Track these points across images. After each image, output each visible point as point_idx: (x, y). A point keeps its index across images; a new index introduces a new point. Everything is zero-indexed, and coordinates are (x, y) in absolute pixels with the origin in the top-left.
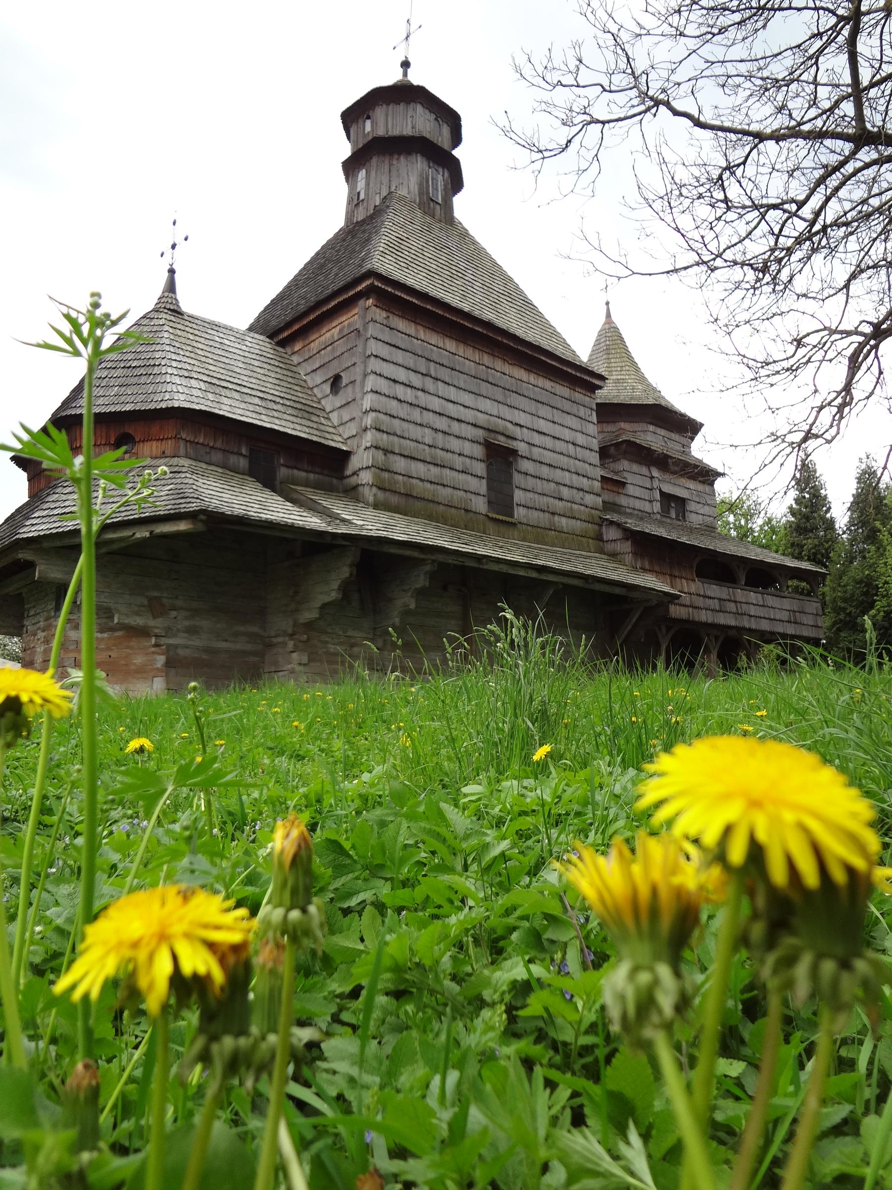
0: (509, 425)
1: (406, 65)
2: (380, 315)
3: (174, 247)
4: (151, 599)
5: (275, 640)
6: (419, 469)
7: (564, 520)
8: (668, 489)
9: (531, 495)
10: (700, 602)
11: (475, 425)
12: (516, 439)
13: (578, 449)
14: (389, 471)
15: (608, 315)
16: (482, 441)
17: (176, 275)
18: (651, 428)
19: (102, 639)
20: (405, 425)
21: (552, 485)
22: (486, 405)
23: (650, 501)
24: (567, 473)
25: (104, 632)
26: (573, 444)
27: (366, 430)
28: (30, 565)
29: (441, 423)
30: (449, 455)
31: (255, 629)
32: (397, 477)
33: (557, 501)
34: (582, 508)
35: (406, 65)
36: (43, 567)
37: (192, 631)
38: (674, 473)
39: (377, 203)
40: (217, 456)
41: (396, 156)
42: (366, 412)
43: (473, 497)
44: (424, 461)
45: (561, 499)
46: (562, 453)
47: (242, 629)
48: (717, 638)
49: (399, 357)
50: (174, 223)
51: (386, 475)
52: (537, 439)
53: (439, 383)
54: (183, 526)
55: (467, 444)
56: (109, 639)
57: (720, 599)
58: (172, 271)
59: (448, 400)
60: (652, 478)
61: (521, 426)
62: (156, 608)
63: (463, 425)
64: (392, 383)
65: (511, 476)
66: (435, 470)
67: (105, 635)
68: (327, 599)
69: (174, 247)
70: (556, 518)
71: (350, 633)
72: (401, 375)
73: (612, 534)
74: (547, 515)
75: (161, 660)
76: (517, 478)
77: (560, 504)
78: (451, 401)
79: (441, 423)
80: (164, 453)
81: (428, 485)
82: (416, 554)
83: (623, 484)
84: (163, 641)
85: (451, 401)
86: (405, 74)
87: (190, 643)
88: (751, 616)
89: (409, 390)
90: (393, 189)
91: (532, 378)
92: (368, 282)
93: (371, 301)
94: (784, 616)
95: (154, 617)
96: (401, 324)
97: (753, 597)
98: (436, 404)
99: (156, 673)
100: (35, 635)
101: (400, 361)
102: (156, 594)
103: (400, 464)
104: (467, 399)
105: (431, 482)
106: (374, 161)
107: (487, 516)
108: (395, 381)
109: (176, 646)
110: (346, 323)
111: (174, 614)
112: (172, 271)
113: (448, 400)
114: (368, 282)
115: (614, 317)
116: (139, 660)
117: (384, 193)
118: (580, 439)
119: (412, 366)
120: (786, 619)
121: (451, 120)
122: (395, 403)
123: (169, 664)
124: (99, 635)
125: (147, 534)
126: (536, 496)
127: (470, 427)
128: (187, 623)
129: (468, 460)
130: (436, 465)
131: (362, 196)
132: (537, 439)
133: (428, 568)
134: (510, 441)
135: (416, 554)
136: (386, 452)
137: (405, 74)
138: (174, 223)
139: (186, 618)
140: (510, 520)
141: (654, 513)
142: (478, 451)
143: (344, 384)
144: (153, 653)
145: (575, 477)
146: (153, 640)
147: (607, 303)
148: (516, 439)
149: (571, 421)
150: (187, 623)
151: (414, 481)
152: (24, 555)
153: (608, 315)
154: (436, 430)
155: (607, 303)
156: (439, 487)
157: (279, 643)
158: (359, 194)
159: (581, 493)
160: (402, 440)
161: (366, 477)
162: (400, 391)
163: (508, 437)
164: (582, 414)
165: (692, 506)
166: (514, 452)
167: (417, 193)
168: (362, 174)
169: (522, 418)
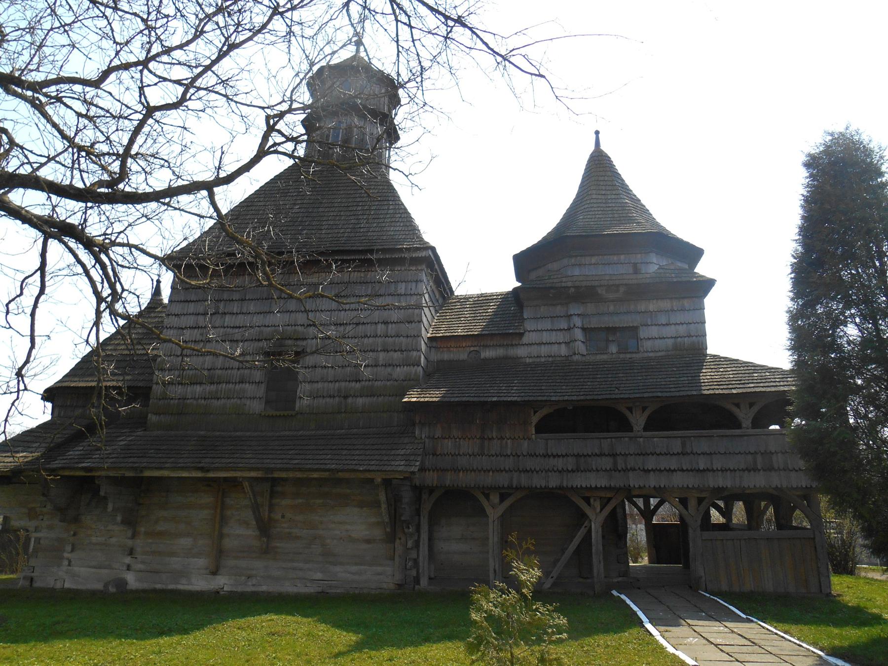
0: (300, 328)
7: (360, 401)
8: (594, 323)
9: (320, 385)
10: (530, 463)
12: (306, 339)
32: (172, 402)
33: (353, 384)
37: (50, 528)
43: (248, 402)
51: (161, 402)
57: (578, 456)
59: (233, 327)
70: (350, 400)
71: (110, 527)
77: (358, 385)
78: (237, 327)
83: (521, 335)
85: (237, 327)
104: (257, 320)
105: (205, 399)
113: (233, 327)
134: (300, 343)
140: (290, 413)
145: (382, 356)
147: (597, 133)
159: (389, 369)
165: (643, 333)
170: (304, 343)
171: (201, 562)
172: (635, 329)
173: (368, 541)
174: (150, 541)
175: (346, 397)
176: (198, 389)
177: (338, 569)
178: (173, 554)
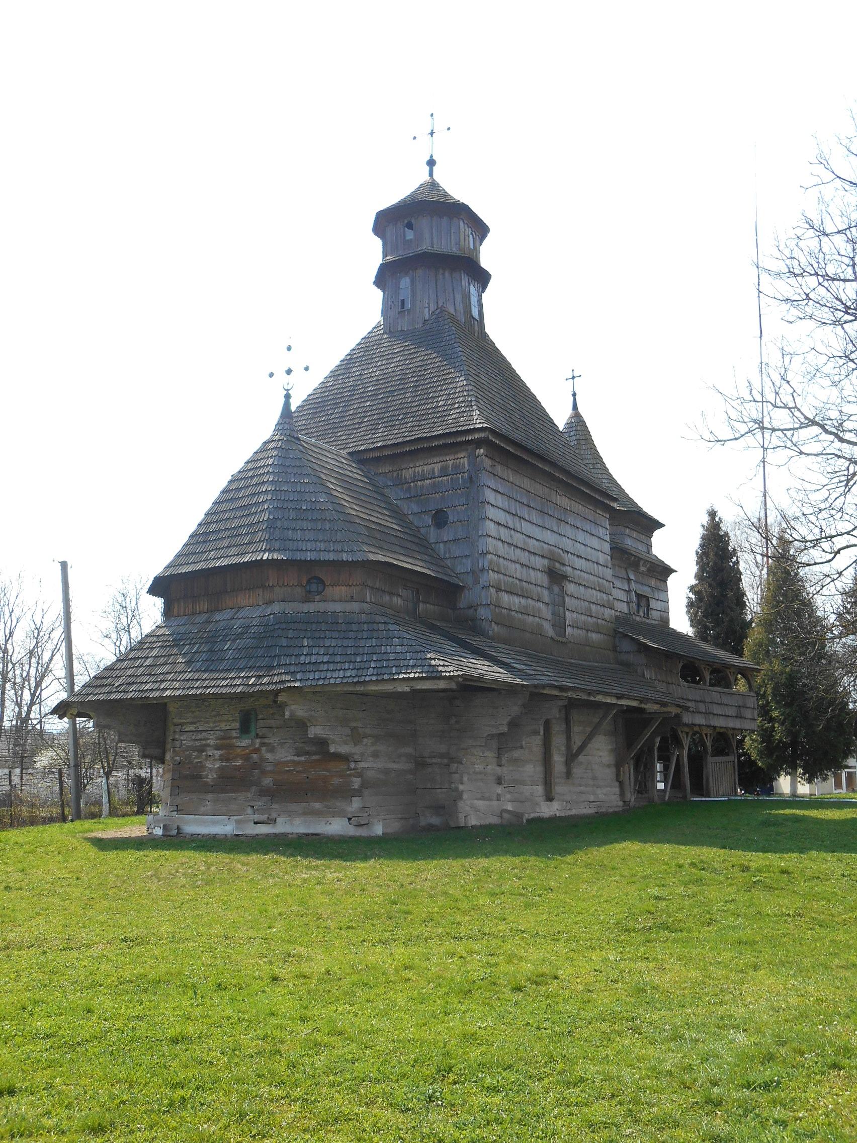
1: (431, 163)
2: (487, 463)
3: (289, 372)
4: (354, 729)
5: (429, 760)
6: (517, 601)
7: (594, 636)
9: (575, 615)
11: (543, 557)
12: (564, 565)
13: (600, 567)
14: (499, 607)
15: (575, 407)
16: (547, 570)
17: (291, 400)
18: (627, 531)
19: (299, 762)
20: (505, 562)
21: (586, 603)
22: (549, 537)
23: (628, 603)
24: (594, 591)
25: (302, 756)
26: (597, 563)
27: (482, 570)
28: (282, 707)
29: (524, 557)
30: (530, 586)
31: (409, 750)
33: (589, 619)
34: (604, 622)
35: (431, 163)
36: (293, 707)
37: (375, 755)
38: (643, 573)
39: (427, 317)
40: (386, 598)
41: (441, 271)
42: (484, 554)
44: (517, 595)
45: (591, 616)
46: (590, 574)
47: (403, 750)
48: (687, 733)
49: (500, 501)
50: (289, 348)
52: (579, 563)
53: (522, 521)
54: (442, 685)
55: (539, 574)
56: (306, 762)
58: (288, 397)
60: (629, 580)
61: (568, 552)
62: (356, 737)
63: (537, 557)
64: (497, 526)
65: (564, 599)
66: (523, 601)
67: (303, 759)
68: (495, 731)
69: (289, 372)
70: (590, 634)
72: (501, 517)
73: (626, 646)
74: (582, 633)
75: (356, 783)
76: (567, 599)
79: (524, 557)
80: (352, 597)
81: (520, 615)
82: (555, 692)
84: (361, 765)
86: (431, 174)
87: (375, 766)
88: (714, 714)
89: (506, 530)
90: (440, 304)
91: (578, 508)
92: (482, 435)
93: (482, 451)
94: (732, 712)
95: (355, 745)
96: (499, 469)
97: (716, 697)
98: (518, 539)
99: (358, 793)
100: (201, 749)
101: (501, 505)
102: (354, 724)
103: (505, 598)
104: (537, 532)
106: (420, 272)
107: (552, 638)
108: (499, 524)
109: (366, 769)
110: (450, 463)
111: (365, 740)
112: (288, 397)
114: (482, 435)
115: (581, 410)
116: (336, 781)
117: (432, 309)
118: (602, 558)
119: (506, 507)
120: (735, 715)
121: (481, 229)
122: (500, 543)
123: (364, 786)
124: (296, 758)
125: (407, 689)
126: (579, 616)
127: (540, 558)
128: (373, 748)
129: (539, 589)
130: (523, 596)
131: (408, 306)
132: (579, 563)
133: (561, 703)
135: (555, 692)
136: (498, 590)
137: (431, 174)
138: (289, 348)
139: (373, 744)
141: (630, 614)
142: (544, 579)
143: (451, 519)
144: (350, 775)
145: (599, 594)
146: (352, 765)
148: (564, 565)
149: (595, 542)
150: (373, 748)
151: (513, 613)
152: (281, 698)
153: (575, 407)
154: (522, 565)
155: (574, 395)
156: (526, 617)
157: (436, 764)
158: (403, 301)
159: (602, 608)
160: (506, 578)
161: (483, 613)
162: (504, 533)
163: (560, 563)
164: (601, 535)
166: (565, 577)
167: (462, 311)
168: (405, 282)
169: (567, 544)
170: (564, 569)
171: (540, 789)
172: (648, 599)
173: (609, 766)
174: (511, 768)
175: (587, 631)
176: (516, 600)
177: (599, 791)
178: (523, 783)
